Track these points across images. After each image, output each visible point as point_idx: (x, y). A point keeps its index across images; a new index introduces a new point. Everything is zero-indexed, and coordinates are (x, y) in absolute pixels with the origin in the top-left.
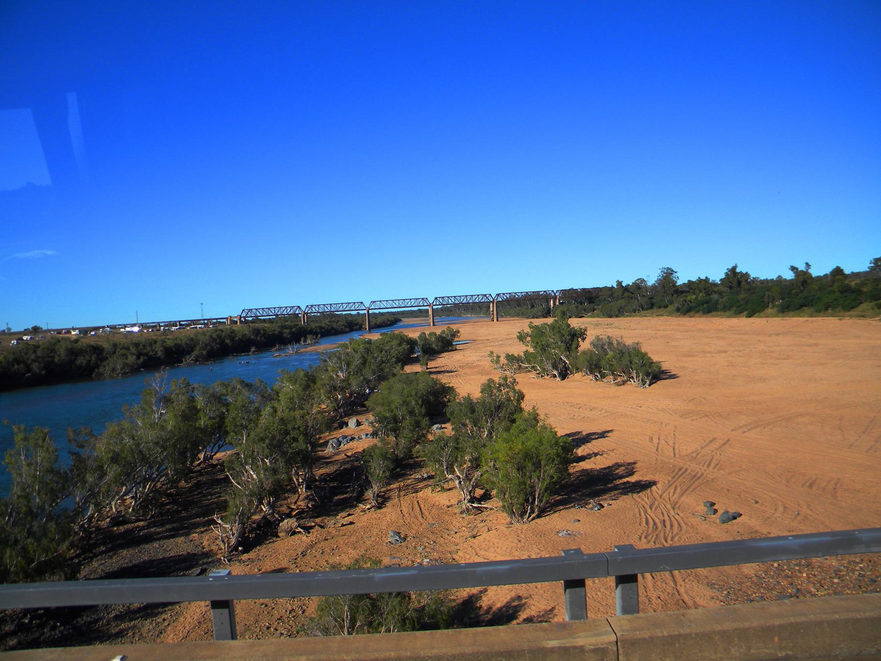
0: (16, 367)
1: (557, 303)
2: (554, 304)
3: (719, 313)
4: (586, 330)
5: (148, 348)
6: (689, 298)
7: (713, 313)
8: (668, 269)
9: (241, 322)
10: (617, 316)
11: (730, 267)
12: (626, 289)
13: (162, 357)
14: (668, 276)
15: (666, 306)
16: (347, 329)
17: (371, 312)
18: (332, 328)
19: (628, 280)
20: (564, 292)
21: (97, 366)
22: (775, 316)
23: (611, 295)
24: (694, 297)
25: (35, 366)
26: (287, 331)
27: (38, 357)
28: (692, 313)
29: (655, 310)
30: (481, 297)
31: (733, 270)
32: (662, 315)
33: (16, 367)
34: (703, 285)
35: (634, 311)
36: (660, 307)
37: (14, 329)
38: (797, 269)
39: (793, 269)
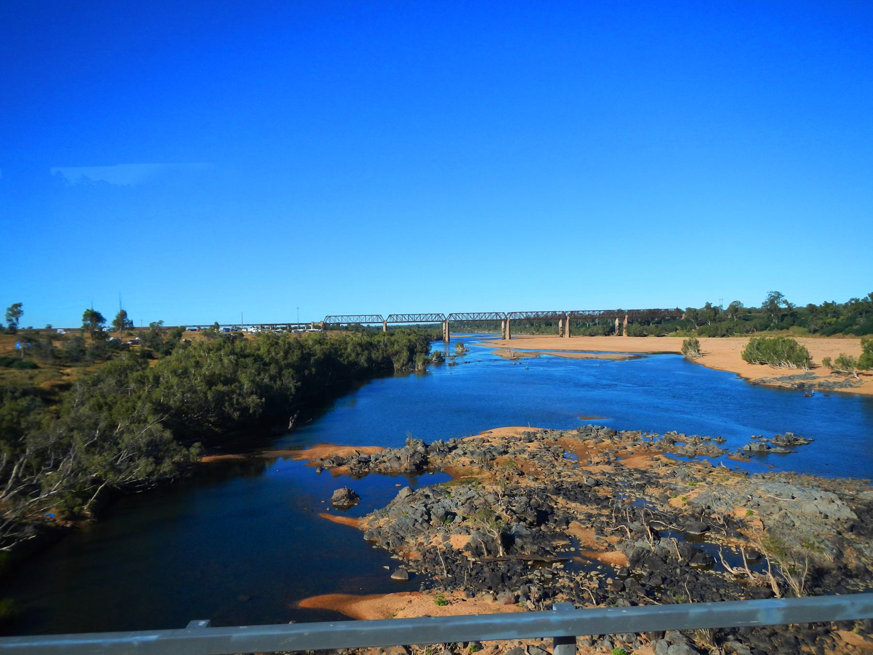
1: (625, 322)
2: (620, 325)
6: (828, 321)
10: (723, 336)
12: (716, 310)
14: (775, 297)
34: (829, 309)
35: (747, 332)
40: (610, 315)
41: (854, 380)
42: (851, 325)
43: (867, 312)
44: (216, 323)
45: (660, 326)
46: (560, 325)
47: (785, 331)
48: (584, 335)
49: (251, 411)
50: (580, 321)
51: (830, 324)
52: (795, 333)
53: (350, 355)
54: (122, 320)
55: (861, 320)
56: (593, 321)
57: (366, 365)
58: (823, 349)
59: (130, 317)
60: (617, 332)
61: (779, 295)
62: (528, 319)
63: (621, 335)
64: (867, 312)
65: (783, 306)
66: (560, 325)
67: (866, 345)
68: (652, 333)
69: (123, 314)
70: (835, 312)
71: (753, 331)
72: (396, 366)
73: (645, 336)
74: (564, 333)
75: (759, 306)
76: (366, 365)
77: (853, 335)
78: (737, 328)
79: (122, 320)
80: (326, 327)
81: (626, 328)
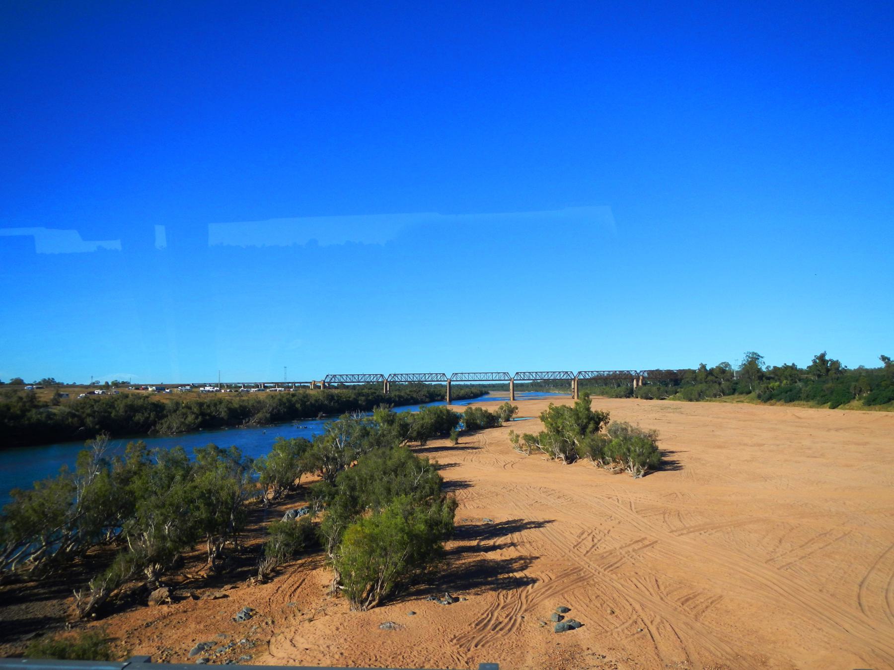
0: (70, 420)
1: (640, 384)
2: (637, 384)
3: (802, 402)
4: (608, 414)
5: (213, 408)
6: (771, 385)
7: (796, 402)
8: (754, 353)
9: (324, 386)
10: (697, 400)
11: (819, 355)
13: (226, 418)
14: (753, 360)
15: (750, 392)
16: (427, 400)
17: (452, 383)
18: (412, 398)
19: (712, 364)
20: (651, 372)
21: (154, 423)
22: (860, 409)
23: (695, 379)
24: (777, 383)
25: (89, 420)
26: (363, 398)
27: (94, 412)
28: (773, 401)
29: (736, 396)
30: (550, 375)
31: (822, 358)
32: (742, 402)
33: (70, 420)
34: (790, 372)
35: (715, 396)
36: (741, 393)
38: (889, 359)
39: (884, 358)
73: (651, 399)
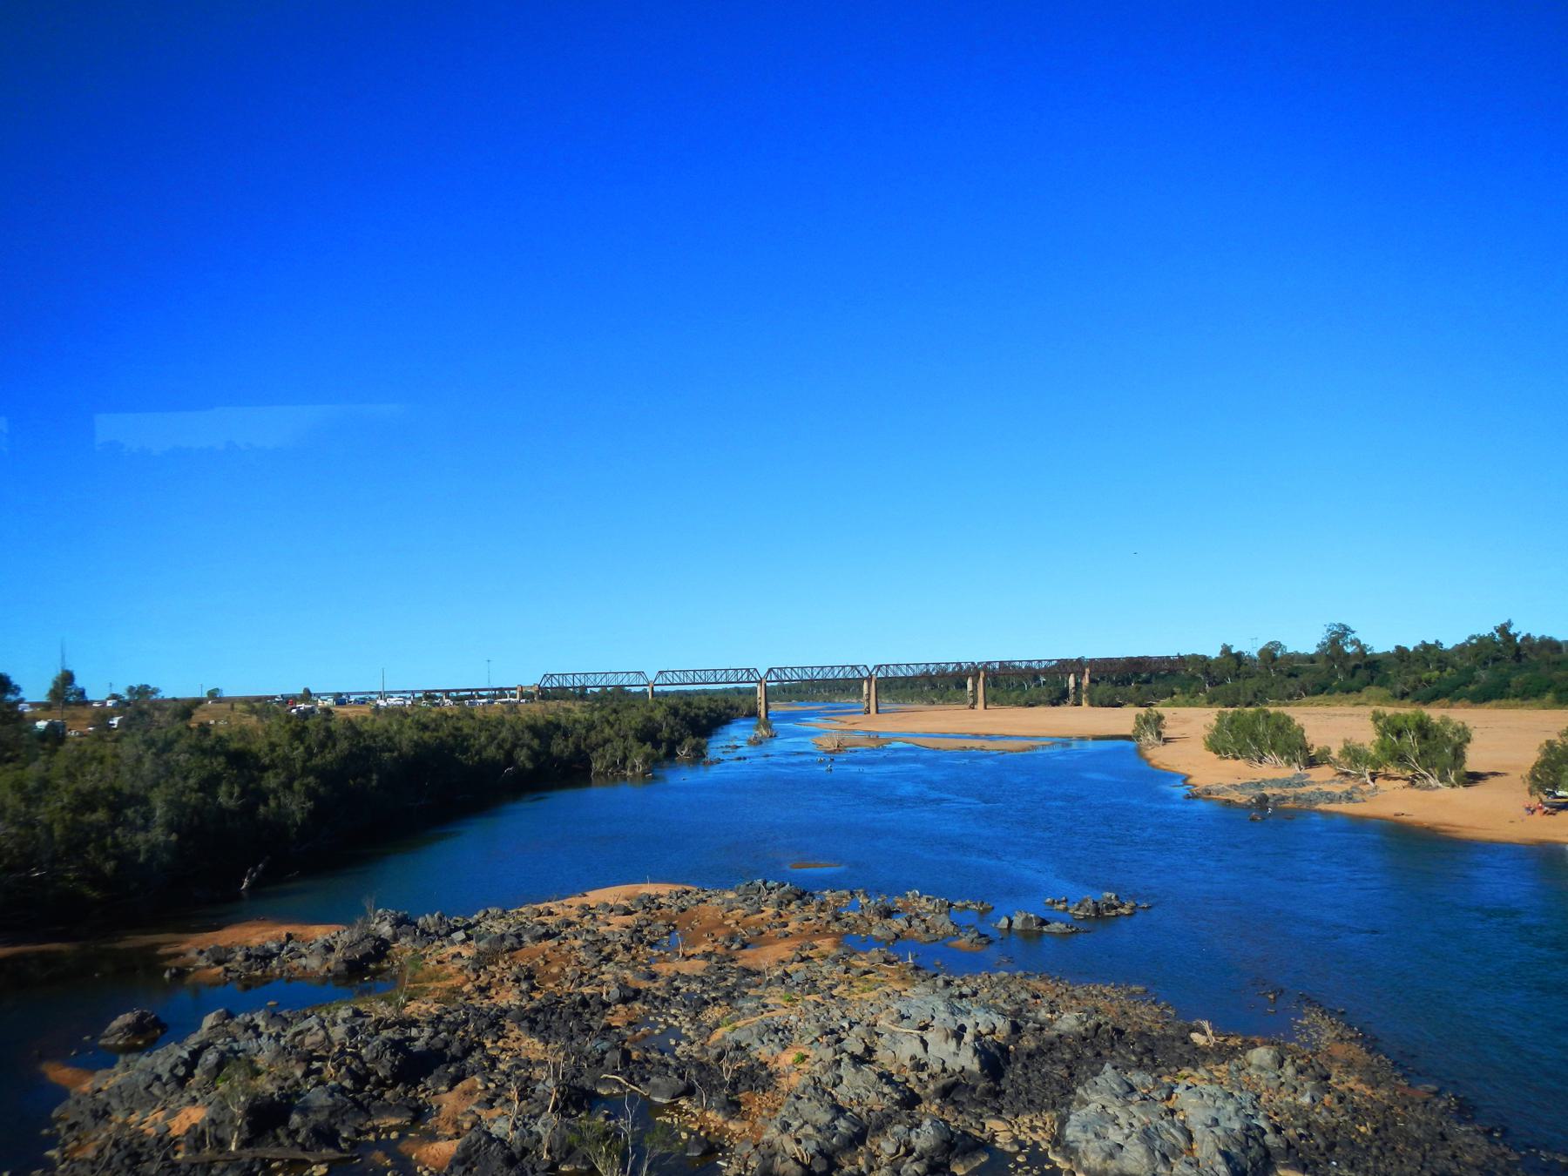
1: (1086, 681)
2: (1078, 685)
3: (1511, 702)
6: (1426, 676)
7: (1494, 702)
8: (1340, 625)
11: (1498, 625)
14: (1339, 635)
19: (1249, 645)
25: (522, 755)
34: (1429, 654)
35: (1290, 697)
37: (226, 694)
40: (1065, 666)
41: (1365, 788)
42: (1466, 684)
43: (1495, 660)
44: (307, 692)
45: (1145, 688)
46: (970, 687)
47: (1353, 695)
48: (1017, 704)
49: (142, 859)
50: (1014, 680)
51: (1429, 682)
52: (1369, 698)
53: (484, 747)
54: (65, 690)
55: (1482, 675)
56: (1036, 678)
57: (529, 765)
58: (1337, 725)
59: (79, 683)
60: (1072, 697)
61: (1345, 630)
62: (927, 677)
63: (1079, 704)
64: (1495, 660)
65: (1349, 649)
66: (970, 687)
67: (1381, 723)
68: (1130, 701)
69: (67, 678)
70: (1439, 661)
71: (1300, 696)
72: (597, 766)
73: (1119, 705)
74: (975, 702)
75: (1312, 650)
76: (529, 765)
77: (1468, 702)
78: (1272, 691)
79: (65, 690)
80: (544, 694)
81: (1088, 690)
